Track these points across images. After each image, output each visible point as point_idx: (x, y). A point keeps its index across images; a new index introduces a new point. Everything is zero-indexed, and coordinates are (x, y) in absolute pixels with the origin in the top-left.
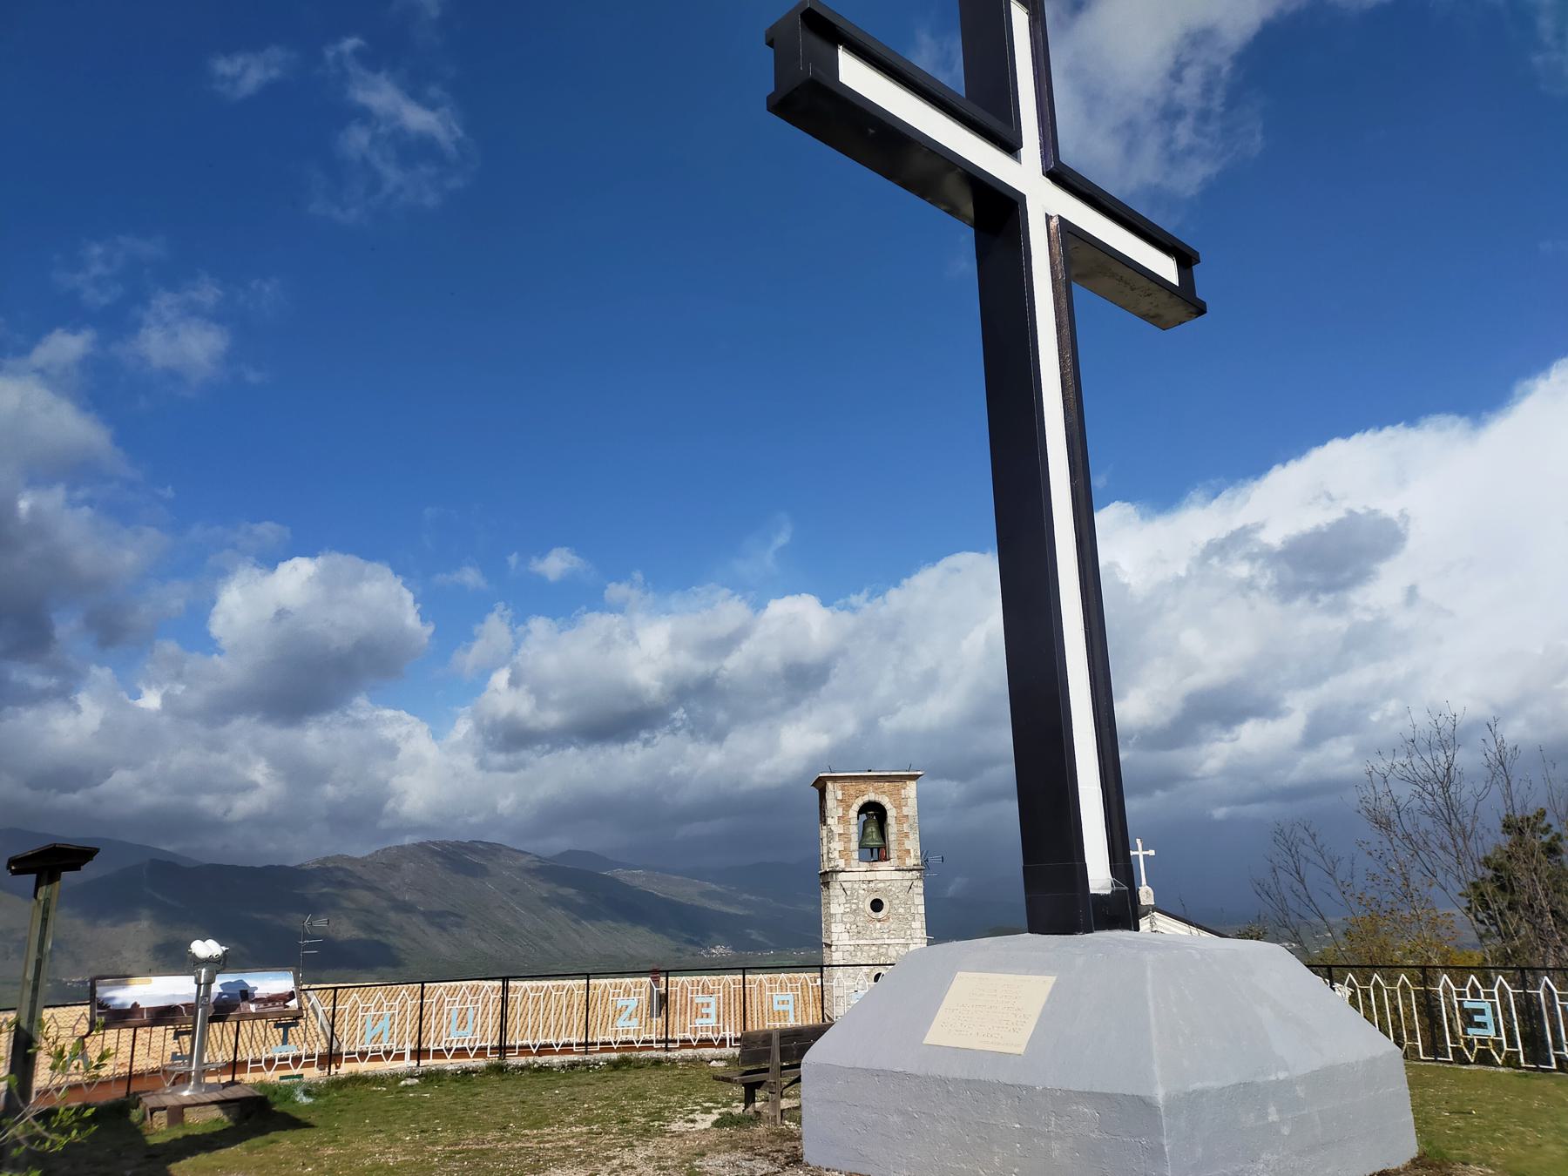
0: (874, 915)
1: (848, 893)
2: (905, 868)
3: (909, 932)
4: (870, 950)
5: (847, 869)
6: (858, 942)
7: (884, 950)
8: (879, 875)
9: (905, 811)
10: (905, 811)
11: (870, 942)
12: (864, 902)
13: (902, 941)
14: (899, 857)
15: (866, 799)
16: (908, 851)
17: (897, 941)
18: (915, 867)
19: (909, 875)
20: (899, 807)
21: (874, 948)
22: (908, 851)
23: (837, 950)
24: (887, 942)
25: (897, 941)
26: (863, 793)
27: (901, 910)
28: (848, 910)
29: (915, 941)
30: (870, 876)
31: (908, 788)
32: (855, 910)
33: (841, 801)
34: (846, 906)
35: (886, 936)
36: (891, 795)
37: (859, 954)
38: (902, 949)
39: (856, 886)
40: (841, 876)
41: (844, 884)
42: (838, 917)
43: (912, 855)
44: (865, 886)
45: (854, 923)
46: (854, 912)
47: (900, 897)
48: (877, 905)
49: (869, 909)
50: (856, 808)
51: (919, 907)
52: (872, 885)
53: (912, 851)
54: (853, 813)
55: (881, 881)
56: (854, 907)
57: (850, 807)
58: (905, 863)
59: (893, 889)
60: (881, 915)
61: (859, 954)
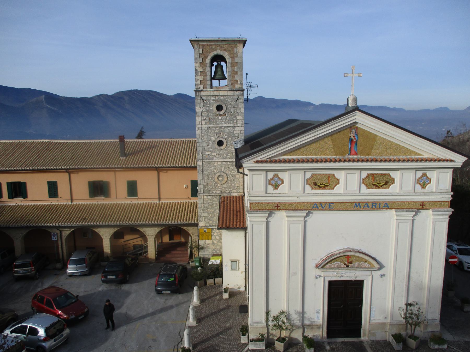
0: (218, 113)
1: (205, 102)
2: (235, 89)
3: (235, 121)
4: (215, 129)
5: (204, 90)
6: (209, 126)
7: (222, 130)
8: (221, 93)
9: (236, 60)
10: (236, 60)
11: (216, 126)
12: (213, 106)
13: (232, 125)
14: (232, 84)
15: (215, 53)
16: (237, 81)
17: (229, 125)
18: (240, 89)
19: (237, 93)
20: (233, 58)
21: (217, 129)
22: (237, 81)
23: (199, 130)
24: (224, 125)
25: (229, 125)
26: (214, 50)
27: (232, 110)
28: (205, 110)
29: (238, 125)
30: (216, 93)
31: (238, 47)
32: (208, 110)
33: (201, 54)
34: (203, 108)
35: (224, 123)
36: (229, 51)
37: (210, 131)
38: (231, 129)
39: (209, 98)
40: (203, 93)
41: (203, 97)
42: (200, 114)
43: (239, 82)
44: (213, 98)
45: (208, 116)
46: (207, 111)
47: (232, 104)
48: (219, 108)
49: (215, 110)
50: (209, 58)
51: (241, 109)
52: (217, 98)
53: (239, 81)
54: (208, 61)
55: (222, 96)
56: (208, 108)
57: (206, 57)
58: (235, 87)
59: (229, 100)
60: (222, 112)
61: (210, 131)
